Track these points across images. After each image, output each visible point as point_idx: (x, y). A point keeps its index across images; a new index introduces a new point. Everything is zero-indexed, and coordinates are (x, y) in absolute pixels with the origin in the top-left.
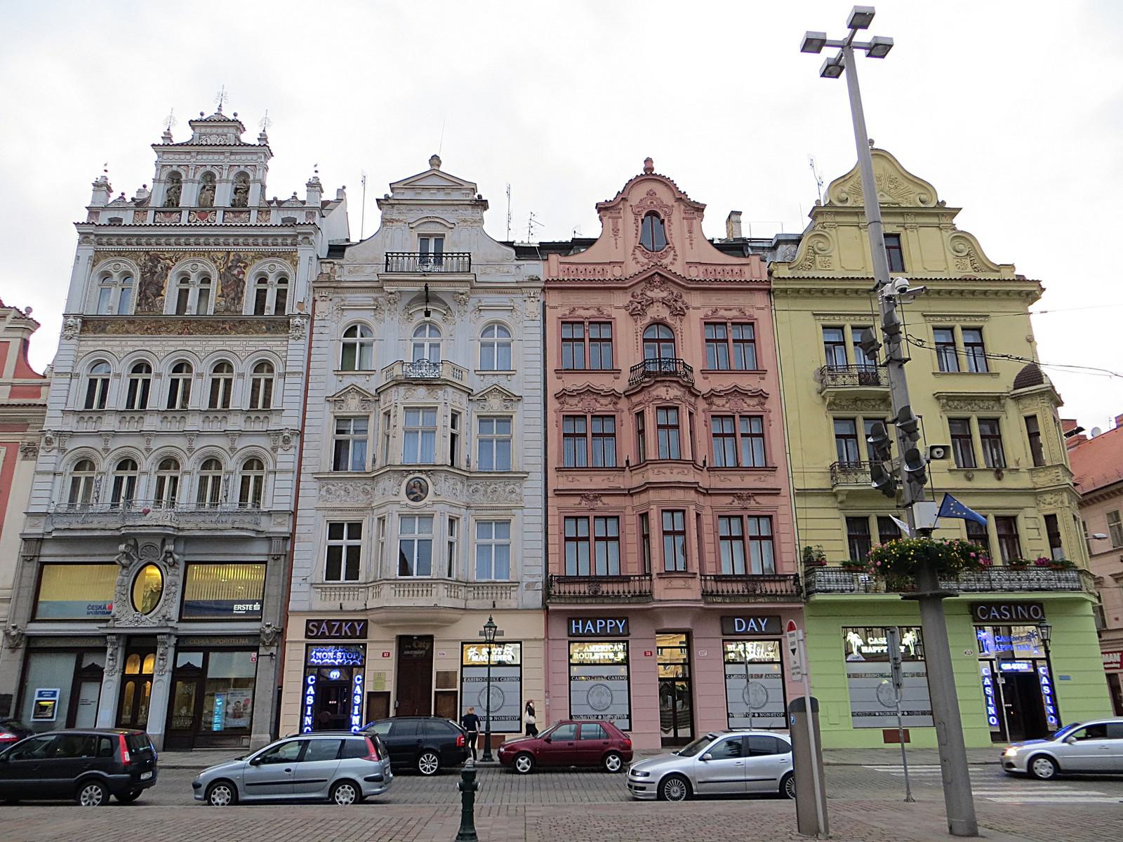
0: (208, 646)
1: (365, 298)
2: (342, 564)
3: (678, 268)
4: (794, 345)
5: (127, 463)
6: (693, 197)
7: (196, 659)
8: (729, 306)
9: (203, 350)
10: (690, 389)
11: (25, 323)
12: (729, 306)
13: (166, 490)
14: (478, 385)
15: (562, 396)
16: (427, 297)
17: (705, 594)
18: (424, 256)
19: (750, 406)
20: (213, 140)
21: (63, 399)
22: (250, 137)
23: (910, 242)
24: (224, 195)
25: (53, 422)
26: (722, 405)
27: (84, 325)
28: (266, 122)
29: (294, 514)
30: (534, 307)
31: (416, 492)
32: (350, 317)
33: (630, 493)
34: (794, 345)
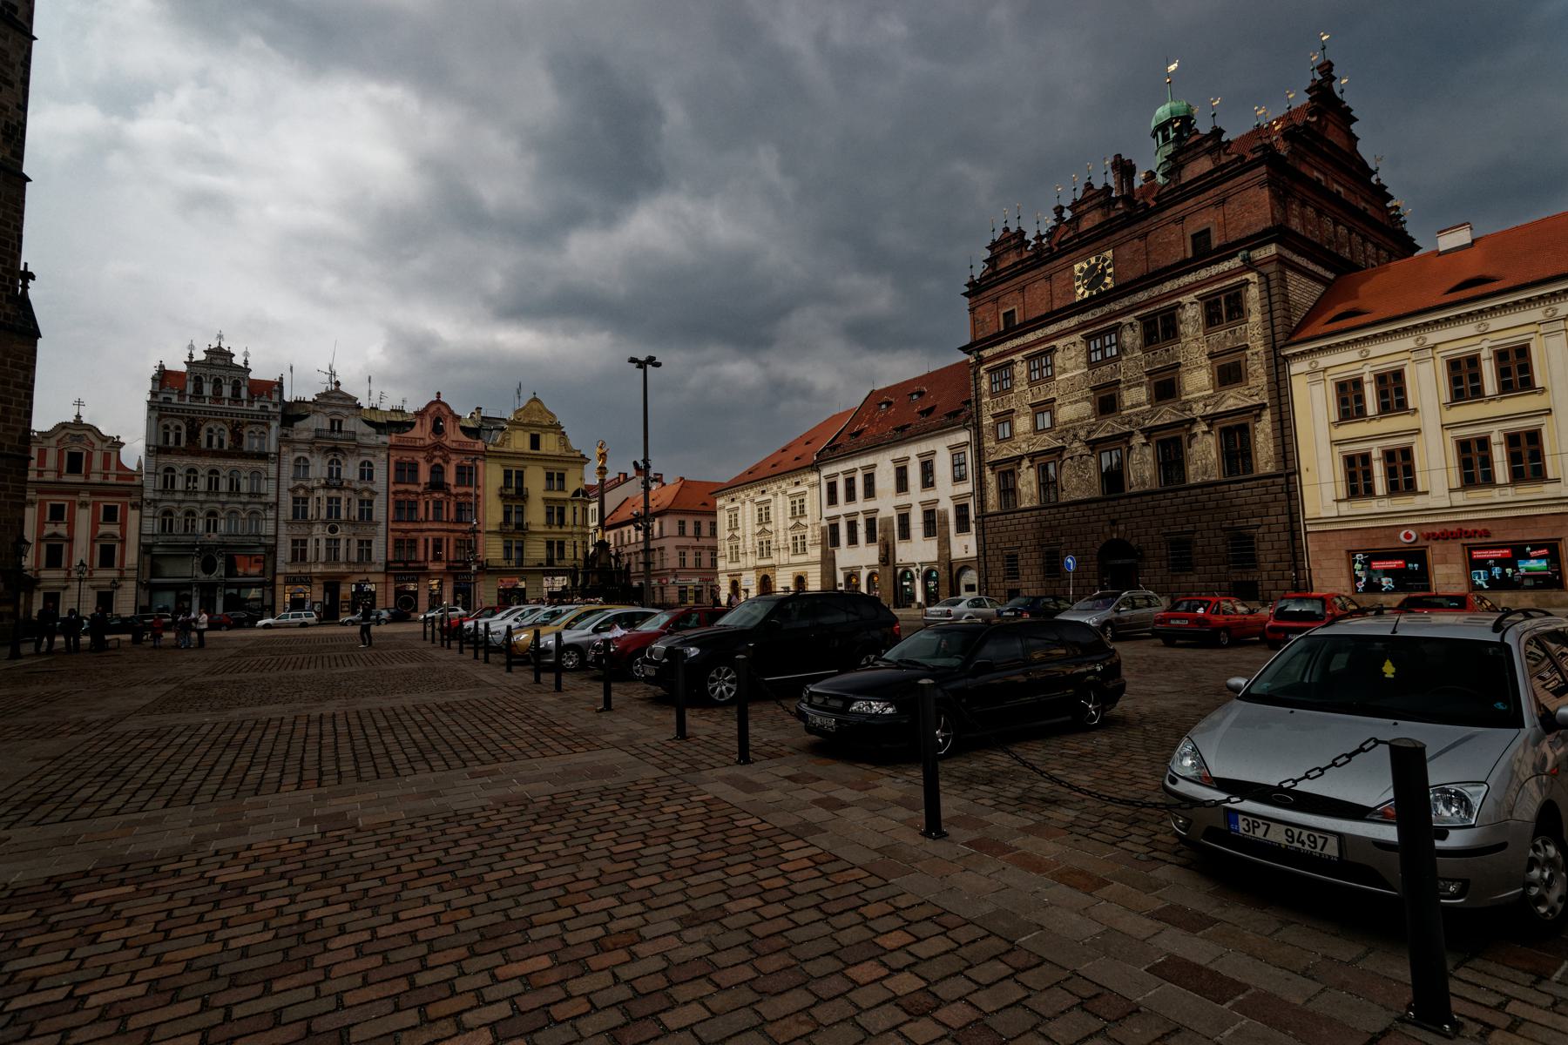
1: (306, 447)
2: (299, 554)
3: (447, 443)
4: (492, 477)
6: (457, 412)
7: (235, 591)
10: (450, 494)
11: (117, 444)
14: (358, 486)
15: (395, 493)
17: (448, 568)
18: (332, 430)
20: (219, 362)
23: (543, 439)
24: (227, 391)
25: (148, 495)
28: (246, 354)
29: (276, 536)
30: (384, 456)
31: (333, 530)
32: (298, 454)
33: (421, 531)
34: (492, 477)
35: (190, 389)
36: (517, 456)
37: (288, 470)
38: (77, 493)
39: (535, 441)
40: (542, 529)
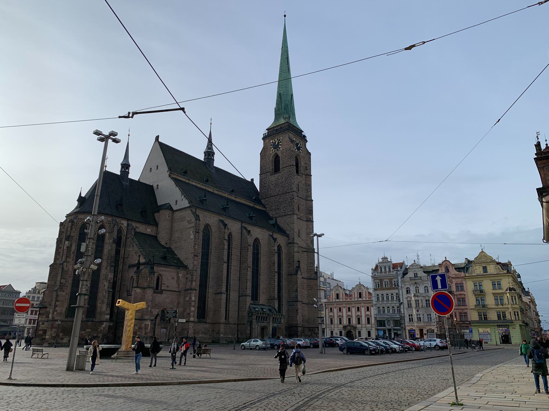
0: (397, 330)
2: (411, 320)
5: (383, 308)
8: (459, 281)
9: (389, 292)
12: (459, 281)
13: (389, 311)
14: (424, 295)
16: (416, 283)
19: (463, 296)
21: (374, 299)
22: (389, 260)
23: (488, 268)
24: (387, 270)
25: (374, 303)
26: (459, 297)
27: (375, 290)
32: (407, 286)
34: (469, 286)
35: (379, 271)
36: (478, 276)
37: (405, 291)
38: (361, 303)
39: (485, 268)
40: (494, 307)
